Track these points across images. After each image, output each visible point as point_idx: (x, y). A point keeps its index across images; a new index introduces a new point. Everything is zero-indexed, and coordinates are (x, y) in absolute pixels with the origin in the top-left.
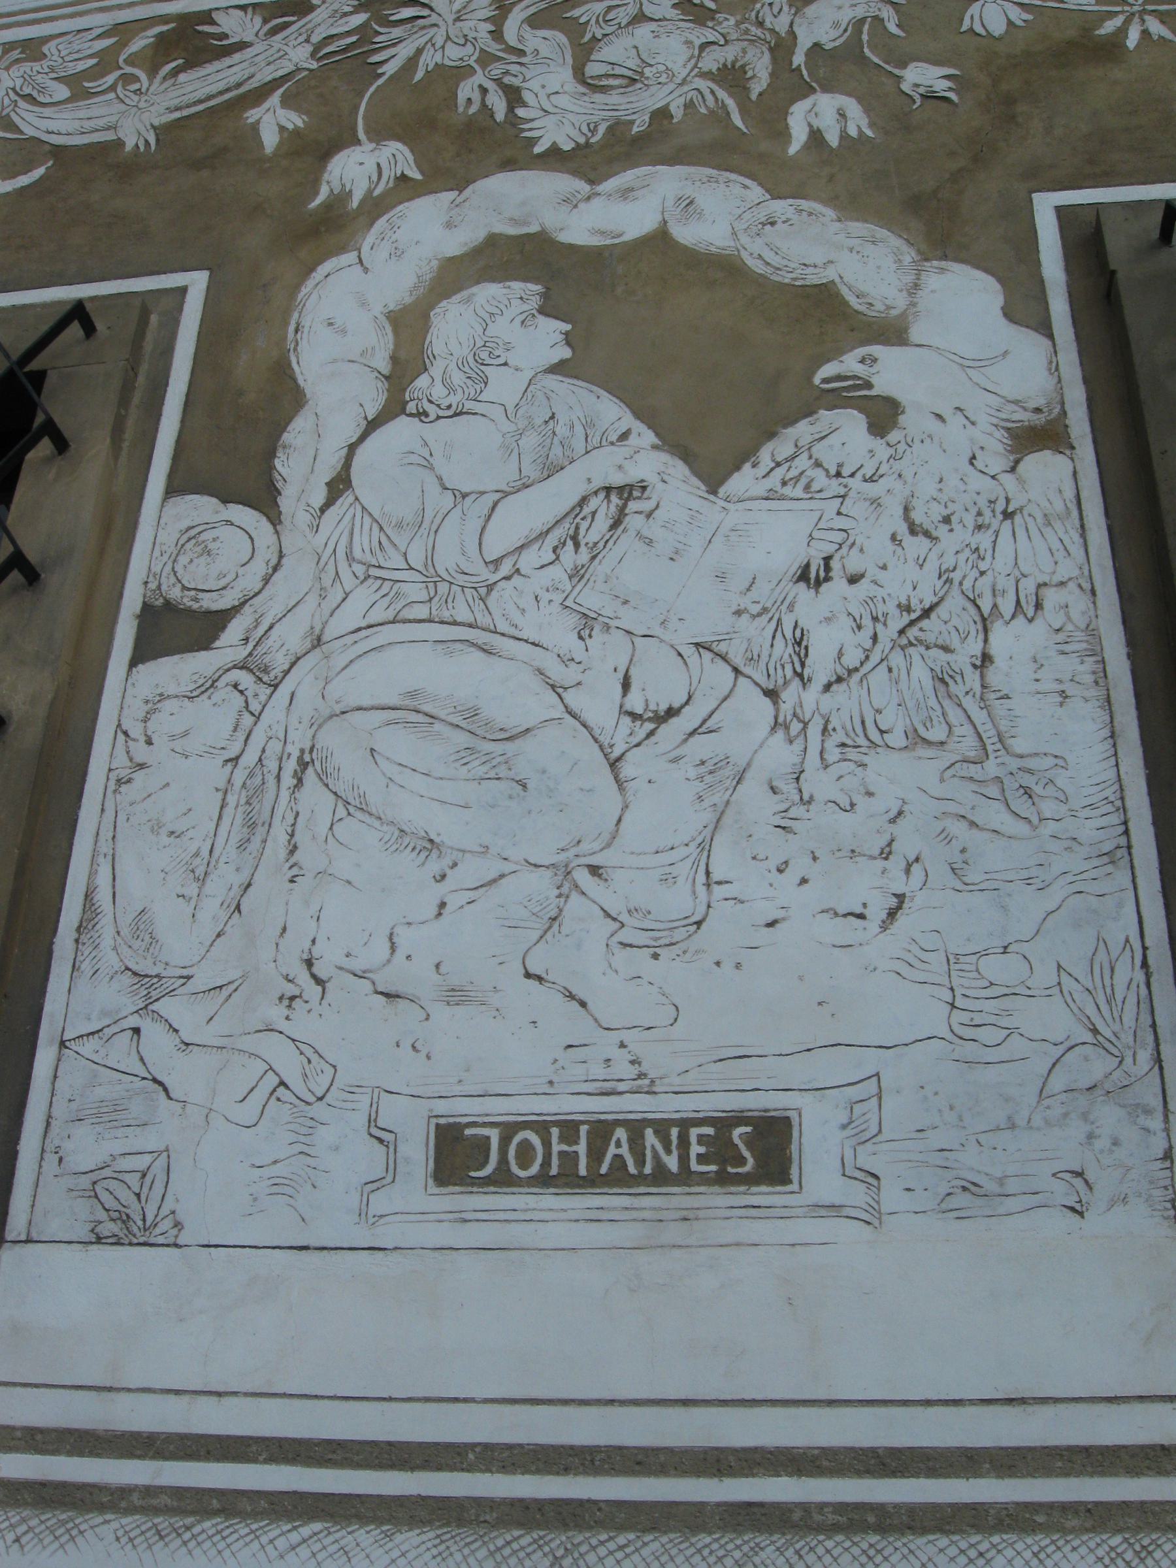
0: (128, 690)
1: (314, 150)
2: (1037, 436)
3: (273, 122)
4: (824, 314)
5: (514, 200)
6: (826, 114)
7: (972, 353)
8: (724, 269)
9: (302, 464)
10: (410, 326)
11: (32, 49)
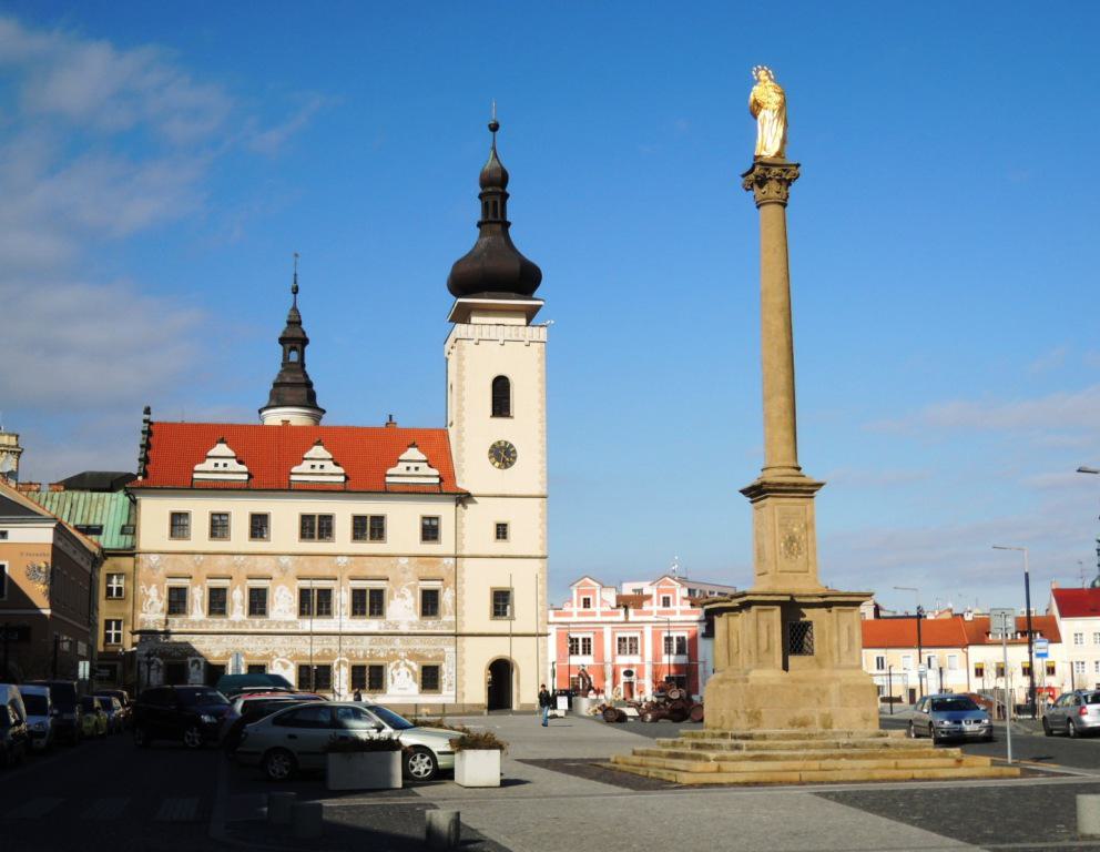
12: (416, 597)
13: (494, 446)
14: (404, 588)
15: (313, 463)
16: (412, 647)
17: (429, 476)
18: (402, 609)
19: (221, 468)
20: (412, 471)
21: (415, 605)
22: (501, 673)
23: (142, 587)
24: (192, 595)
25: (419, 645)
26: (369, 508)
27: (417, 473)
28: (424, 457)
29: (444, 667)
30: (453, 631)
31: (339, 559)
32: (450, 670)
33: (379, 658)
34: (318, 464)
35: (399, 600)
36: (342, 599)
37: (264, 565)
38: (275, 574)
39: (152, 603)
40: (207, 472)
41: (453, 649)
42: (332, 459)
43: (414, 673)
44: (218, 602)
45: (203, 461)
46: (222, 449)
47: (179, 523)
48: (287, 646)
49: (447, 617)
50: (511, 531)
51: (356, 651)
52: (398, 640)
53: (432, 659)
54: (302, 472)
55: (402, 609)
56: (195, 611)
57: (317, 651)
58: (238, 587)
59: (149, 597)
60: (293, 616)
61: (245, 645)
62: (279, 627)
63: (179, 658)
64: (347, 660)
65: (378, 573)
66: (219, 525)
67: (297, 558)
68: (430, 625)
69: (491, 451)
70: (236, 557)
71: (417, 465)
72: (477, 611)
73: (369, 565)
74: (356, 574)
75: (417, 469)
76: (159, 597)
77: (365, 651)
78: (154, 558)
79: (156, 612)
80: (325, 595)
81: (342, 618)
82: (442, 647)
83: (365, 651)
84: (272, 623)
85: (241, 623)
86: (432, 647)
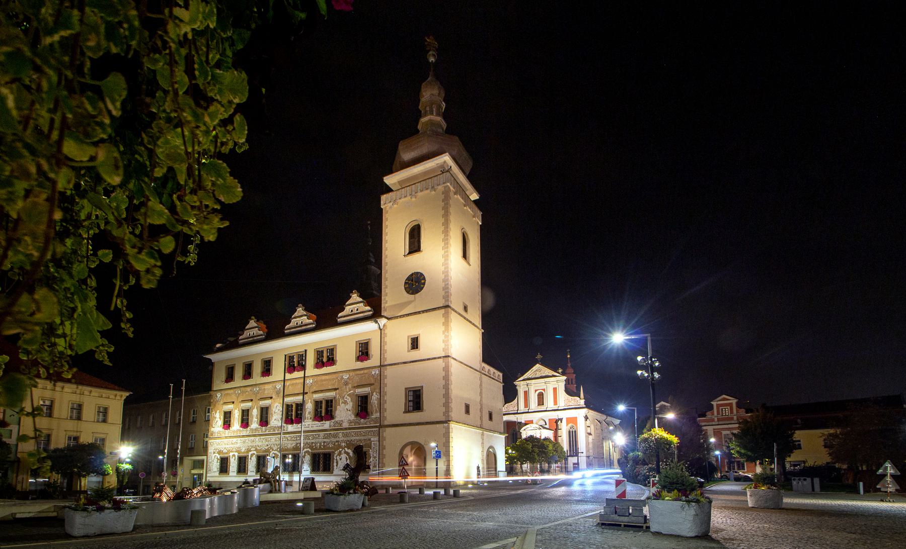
18: (345, 412)
29: (371, 452)
33: (329, 448)
36: (309, 407)
49: (375, 415)
51: (316, 443)
81: (308, 423)
85: (256, 429)
86: (362, 438)
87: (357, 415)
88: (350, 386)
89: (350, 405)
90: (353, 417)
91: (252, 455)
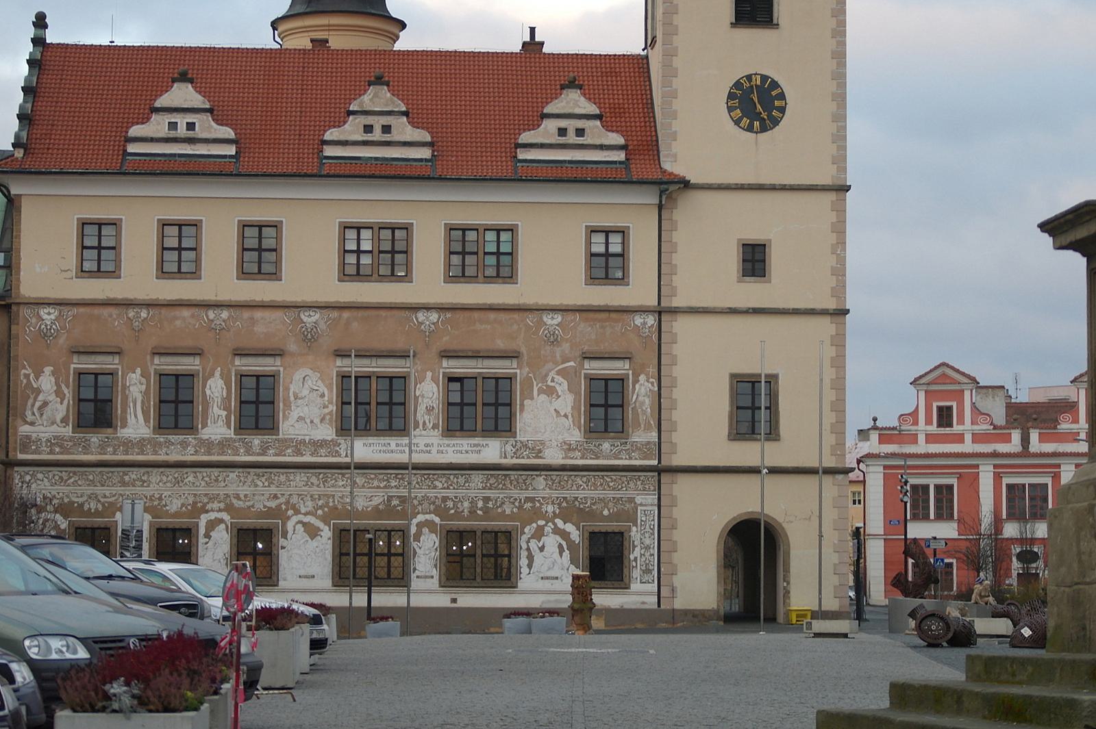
0: (280, 551)
1: (287, 510)
2: (329, 539)
3: (284, 507)
4: (319, 529)
5: (300, 517)
6: (320, 512)
7: (327, 533)
8: (313, 525)
9: (289, 537)
10: (294, 527)
11: (263, 495)
12: (577, 394)
13: (738, 84)
14: (552, 374)
15: (370, 120)
16: (568, 494)
17: (605, 143)
18: (549, 420)
19: (182, 131)
20: (572, 138)
21: (576, 407)
22: (753, 550)
23: (25, 371)
24: (124, 387)
25: (584, 491)
26: (482, 207)
27: (580, 140)
28: (593, 109)
29: (635, 533)
30: (655, 462)
31: (421, 316)
32: (647, 542)
33: (503, 516)
34: (376, 124)
35: (543, 397)
36: (428, 394)
37: (267, 326)
38: (292, 347)
39: (45, 404)
40: (152, 140)
41: (653, 499)
42: (406, 114)
43: (572, 546)
44: (176, 405)
45: (145, 120)
46: (182, 95)
47: (98, 247)
48: (315, 491)
49: (643, 436)
50: (776, 260)
51: (457, 501)
52: (540, 481)
53: (610, 518)
54: (345, 138)
55: (549, 420)
56: (131, 420)
57: (376, 501)
58: (218, 373)
59: (38, 391)
60: (327, 432)
61: (231, 490)
62: (298, 452)
63: (97, 513)
64: (437, 520)
65: (501, 344)
66: (179, 248)
67: (335, 314)
68: (607, 452)
69: (731, 96)
70: (211, 314)
71: (580, 124)
72: (699, 424)
73: (478, 326)
74: (455, 346)
75: (580, 132)
76: (59, 393)
77: (473, 503)
78: (48, 315)
79: (53, 423)
80: (396, 385)
82: (631, 494)
83: (473, 503)
84: (286, 443)
85: (224, 444)
86: (611, 494)
87: (590, 432)
88: (566, 346)
89: (566, 402)
90: (576, 436)
91: (212, 525)
